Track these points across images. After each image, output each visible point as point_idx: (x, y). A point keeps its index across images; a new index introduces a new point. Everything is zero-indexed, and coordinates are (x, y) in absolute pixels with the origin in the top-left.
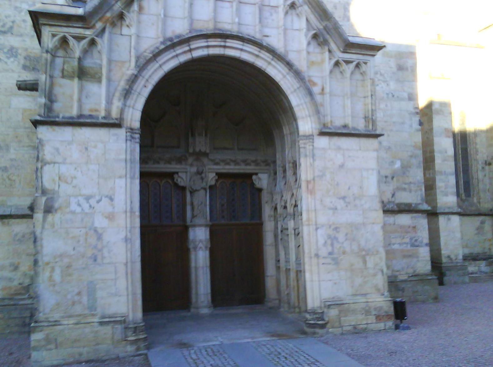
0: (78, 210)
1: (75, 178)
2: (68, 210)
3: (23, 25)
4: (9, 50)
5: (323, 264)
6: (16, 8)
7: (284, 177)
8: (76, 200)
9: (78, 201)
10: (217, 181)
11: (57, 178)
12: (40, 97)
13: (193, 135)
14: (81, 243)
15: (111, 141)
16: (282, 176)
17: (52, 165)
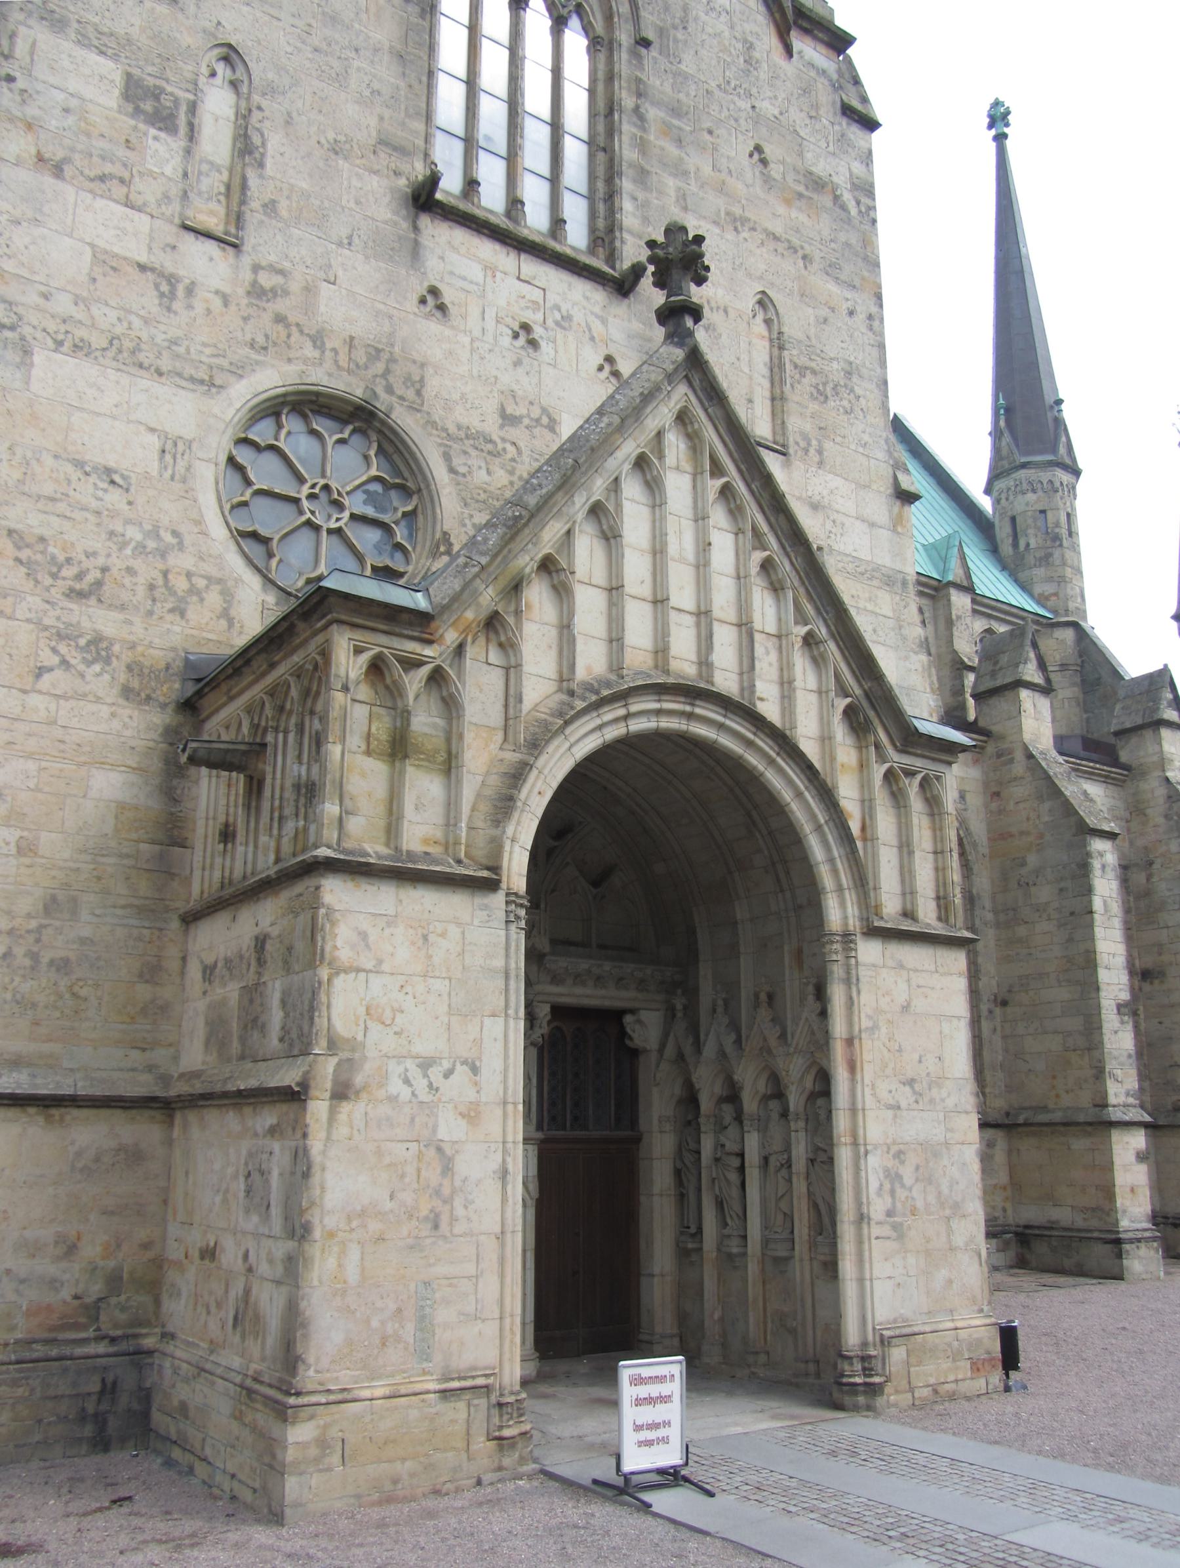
0: (405, 1093)
2: (381, 1094)
3: (127, 581)
4: (89, 643)
5: (877, 1238)
6: (112, 534)
8: (401, 1069)
9: (406, 1070)
11: (362, 1011)
14: (407, 1180)
15: (476, 922)
17: (353, 974)
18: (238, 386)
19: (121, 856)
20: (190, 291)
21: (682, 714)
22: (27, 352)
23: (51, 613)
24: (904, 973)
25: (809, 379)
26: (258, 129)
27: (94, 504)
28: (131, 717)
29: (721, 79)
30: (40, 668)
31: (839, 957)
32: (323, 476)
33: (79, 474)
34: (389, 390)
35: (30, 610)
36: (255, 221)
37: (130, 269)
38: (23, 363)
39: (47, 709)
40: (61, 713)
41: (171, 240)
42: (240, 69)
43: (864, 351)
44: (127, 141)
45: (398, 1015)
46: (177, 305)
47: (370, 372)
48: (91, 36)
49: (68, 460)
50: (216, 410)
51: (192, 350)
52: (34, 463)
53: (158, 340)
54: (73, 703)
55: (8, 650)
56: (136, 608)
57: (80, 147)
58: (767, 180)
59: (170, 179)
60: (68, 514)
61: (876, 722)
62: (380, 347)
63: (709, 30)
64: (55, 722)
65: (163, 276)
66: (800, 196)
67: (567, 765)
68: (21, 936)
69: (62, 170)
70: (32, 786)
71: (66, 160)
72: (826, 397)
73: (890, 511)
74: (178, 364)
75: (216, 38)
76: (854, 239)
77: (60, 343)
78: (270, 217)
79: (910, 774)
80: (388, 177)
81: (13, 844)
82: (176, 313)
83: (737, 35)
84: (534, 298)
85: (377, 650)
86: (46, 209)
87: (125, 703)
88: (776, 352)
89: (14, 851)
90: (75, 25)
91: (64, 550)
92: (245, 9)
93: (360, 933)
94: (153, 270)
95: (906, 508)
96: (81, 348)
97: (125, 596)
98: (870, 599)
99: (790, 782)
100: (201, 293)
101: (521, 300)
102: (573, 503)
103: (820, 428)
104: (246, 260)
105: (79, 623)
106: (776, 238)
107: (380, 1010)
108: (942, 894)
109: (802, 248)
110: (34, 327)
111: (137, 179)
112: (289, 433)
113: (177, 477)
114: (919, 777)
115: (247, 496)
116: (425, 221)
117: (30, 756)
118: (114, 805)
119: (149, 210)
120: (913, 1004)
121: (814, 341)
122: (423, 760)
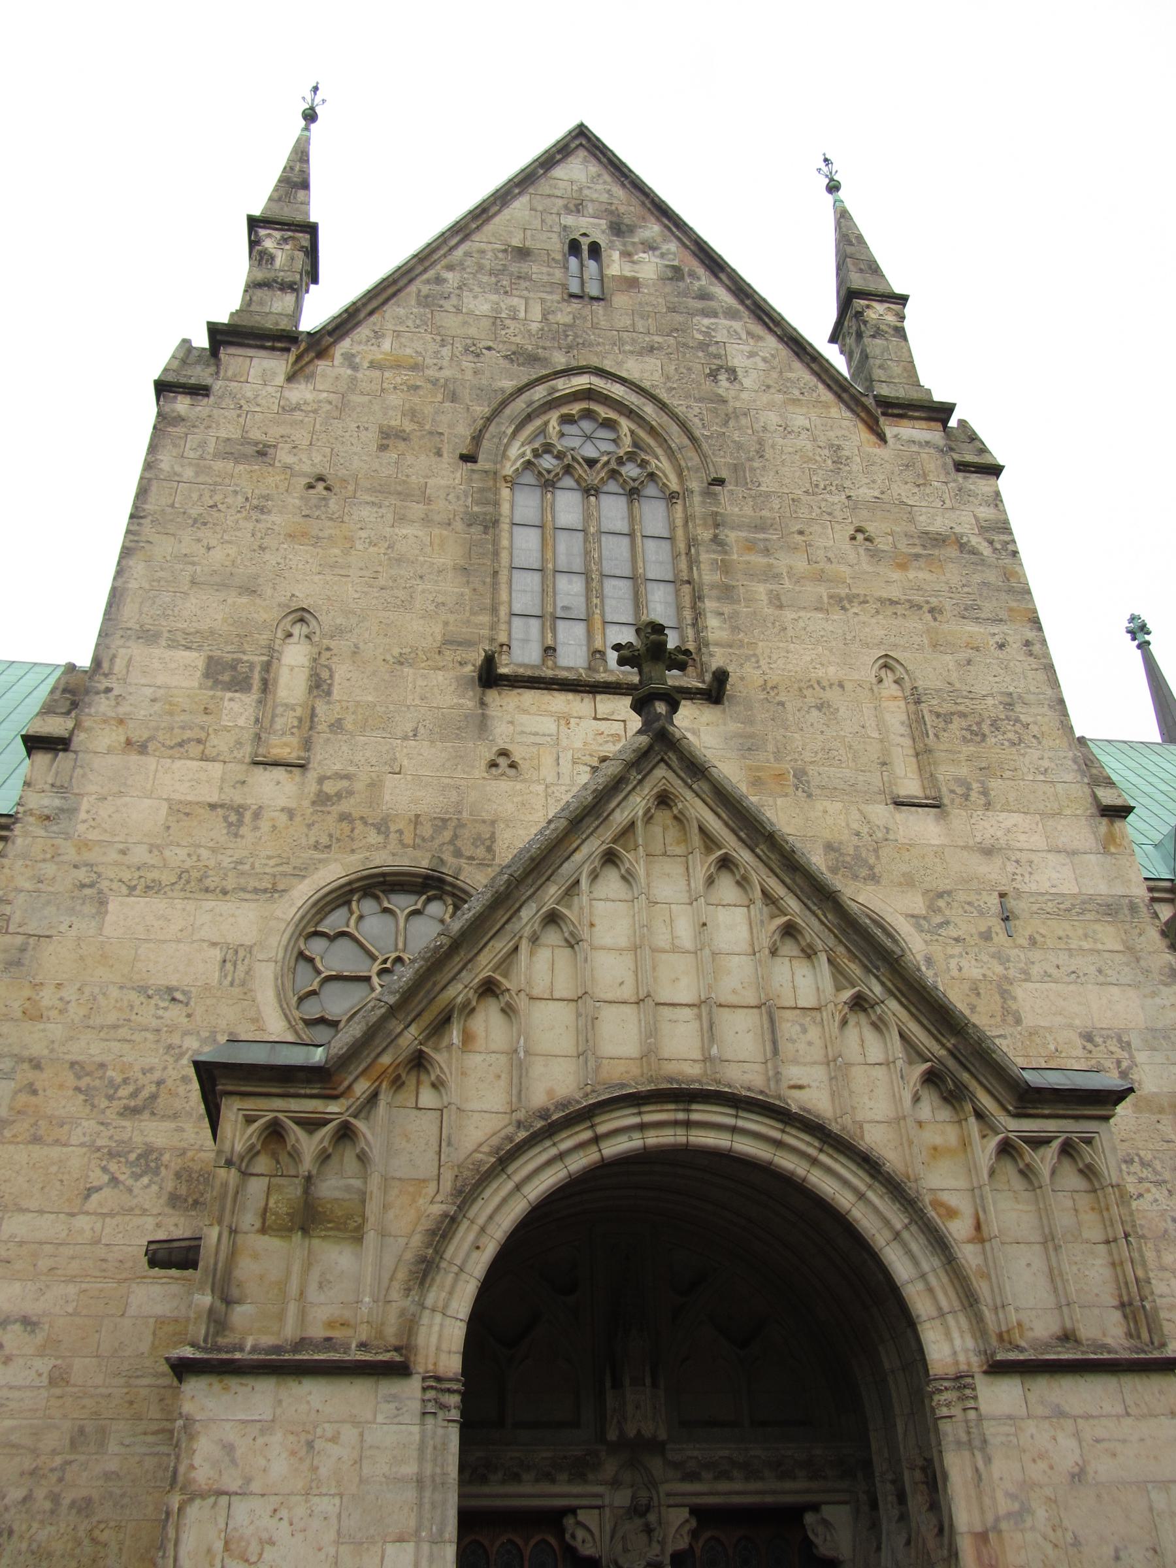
1: (272, 1543)
3: (181, 1090)
4: (138, 1159)
6: (170, 1047)
7: (903, 1517)
10: (694, 1534)
11: (219, 1545)
12: (201, 1290)
13: (617, 1384)
16: (895, 1513)
17: (213, 1499)
18: (300, 887)
19: (157, 1375)
20: (257, 815)
21: (676, 1123)
22: (102, 902)
23: (106, 1133)
24: (1069, 1424)
25: (957, 723)
26: (326, 666)
27: (155, 1023)
28: (176, 1225)
29: (808, 485)
30: (89, 1189)
31: (956, 1411)
32: (396, 950)
33: (142, 999)
34: (458, 854)
35: (84, 1134)
36: (321, 741)
37: (202, 811)
38: (99, 913)
39: (92, 1229)
40: (107, 1230)
41: (241, 777)
42: (313, 623)
43: (1025, 678)
44: (206, 709)
45: (267, 1547)
46: (243, 830)
47: (437, 842)
48: (179, 639)
49: (133, 989)
50: (279, 913)
51: (257, 865)
52: (100, 997)
53: (225, 864)
54: (118, 1219)
55: (60, 1176)
56: (189, 1114)
57: (163, 725)
58: (875, 555)
59: (242, 728)
60: (128, 1038)
61: (973, 1085)
62: (447, 816)
63: (786, 450)
64: (98, 1242)
65: (232, 808)
66: (917, 556)
67: (517, 1209)
68: (44, 1476)
69: (146, 747)
70: (70, 1310)
71: (151, 739)
72: (984, 736)
73: (1094, 833)
74: (242, 881)
75: (289, 607)
76: (992, 577)
77: (134, 888)
78: (336, 733)
79: (1038, 1142)
80: (453, 669)
81: (45, 1375)
82: (242, 837)
83: (821, 444)
84: (613, 732)
85: (272, 1115)
86: (129, 782)
87: (171, 1211)
88: (912, 708)
89: (45, 1380)
90: (166, 635)
91: (122, 1072)
92: (316, 578)
93: (224, 1447)
94: (222, 806)
95: (1118, 824)
96: (152, 888)
97: (178, 1104)
98: (1086, 936)
99: (845, 1183)
100: (266, 814)
101: (598, 737)
102: (520, 918)
103: (981, 769)
104: (312, 775)
105: (131, 1138)
106: (893, 602)
107: (243, 1544)
108: (1125, 1299)
109: (928, 602)
110: (111, 880)
111: (212, 736)
112: (361, 917)
113: (237, 982)
114: (1056, 1144)
115: (315, 986)
116: (492, 696)
117: (71, 1279)
118: (152, 1320)
119: (221, 758)
120: (1090, 1470)
121: (958, 686)
122: (331, 1229)
